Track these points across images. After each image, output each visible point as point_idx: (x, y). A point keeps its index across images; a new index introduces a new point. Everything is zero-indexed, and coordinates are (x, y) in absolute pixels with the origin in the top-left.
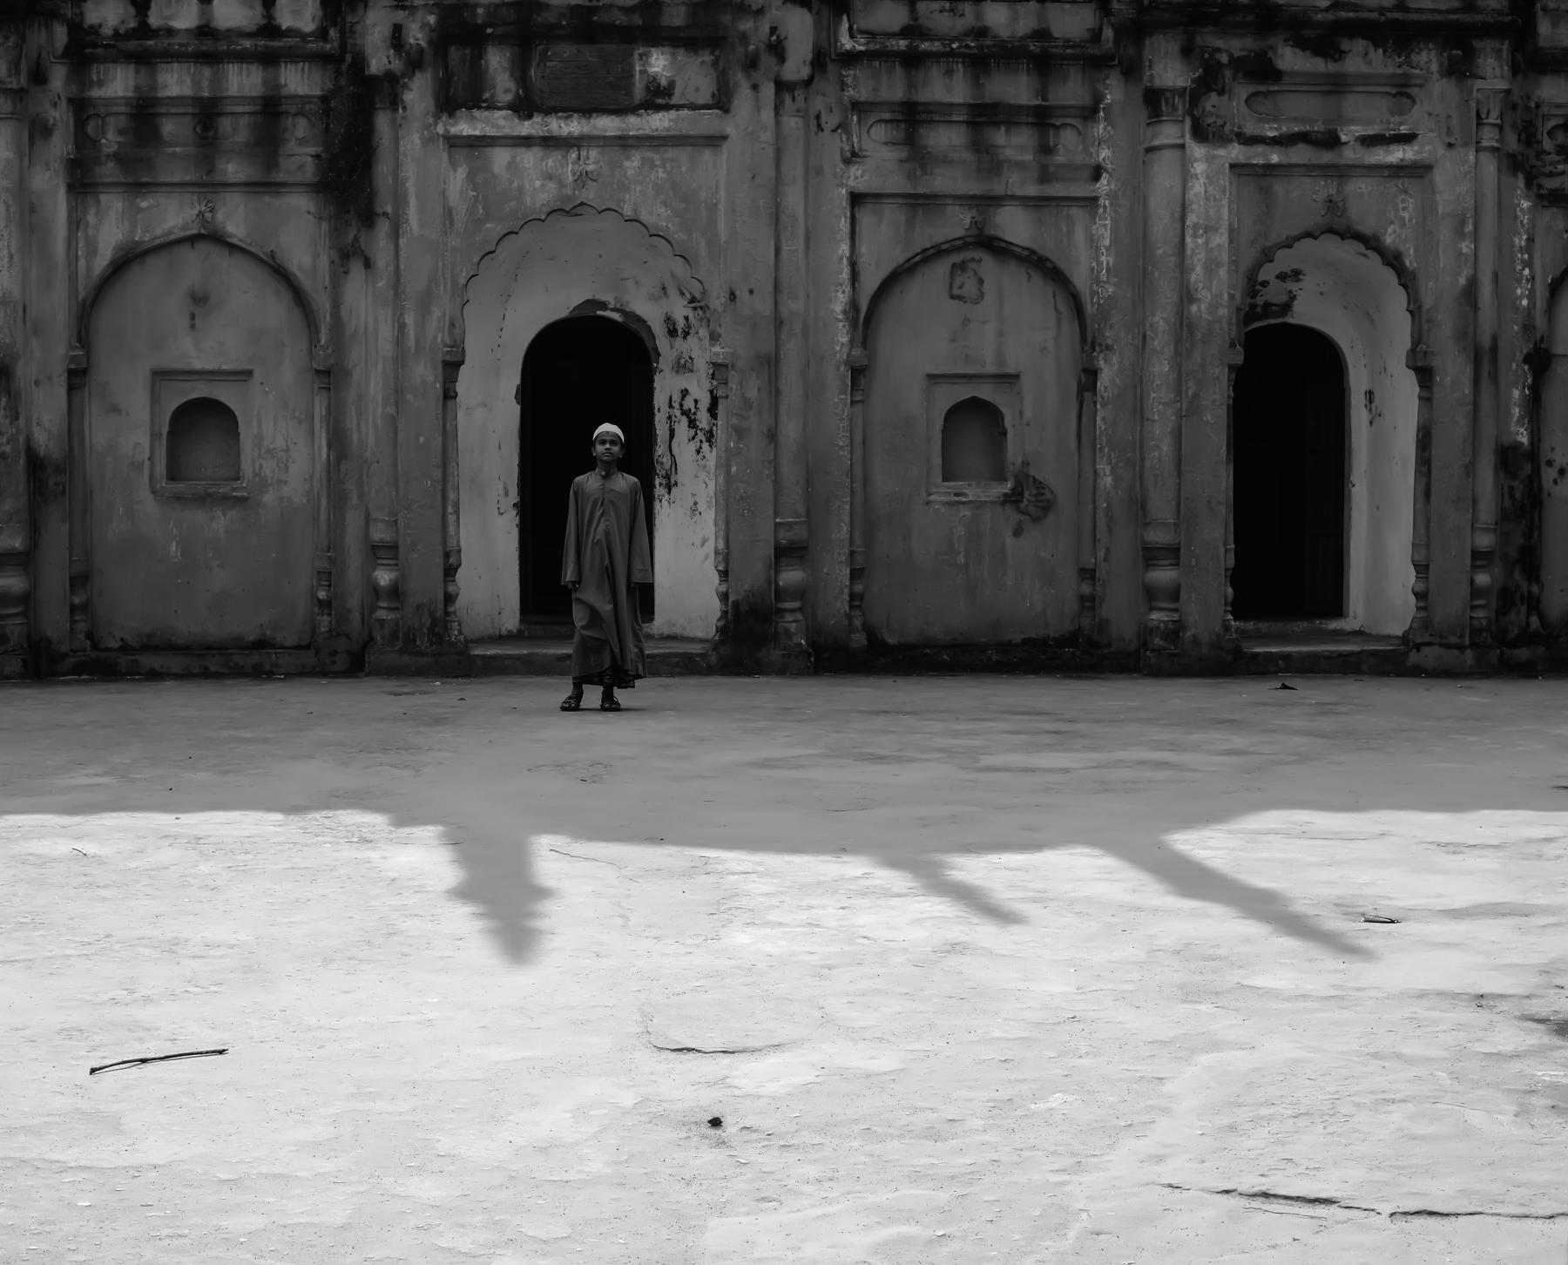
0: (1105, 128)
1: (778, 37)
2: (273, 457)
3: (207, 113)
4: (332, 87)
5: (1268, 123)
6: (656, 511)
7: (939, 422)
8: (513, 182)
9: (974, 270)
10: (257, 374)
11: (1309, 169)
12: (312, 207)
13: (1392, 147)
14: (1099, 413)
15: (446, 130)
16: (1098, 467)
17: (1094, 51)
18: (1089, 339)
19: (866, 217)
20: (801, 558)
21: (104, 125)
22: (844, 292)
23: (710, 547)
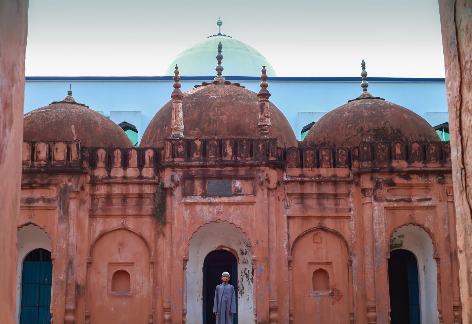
1: (268, 177)
2: (139, 285)
3: (125, 197)
4: (156, 191)
5: (393, 196)
7: (312, 275)
9: (319, 235)
10: (135, 264)
11: (405, 208)
12: (150, 221)
13: (425, 202)
14: (353, 272)
15: (185, 201)
16: (353, 286)
17: (348, 179)
19: (291, 222)
20: (276, 311)
21: (98, 200)
22: (286, 241)
23: (252, 309)
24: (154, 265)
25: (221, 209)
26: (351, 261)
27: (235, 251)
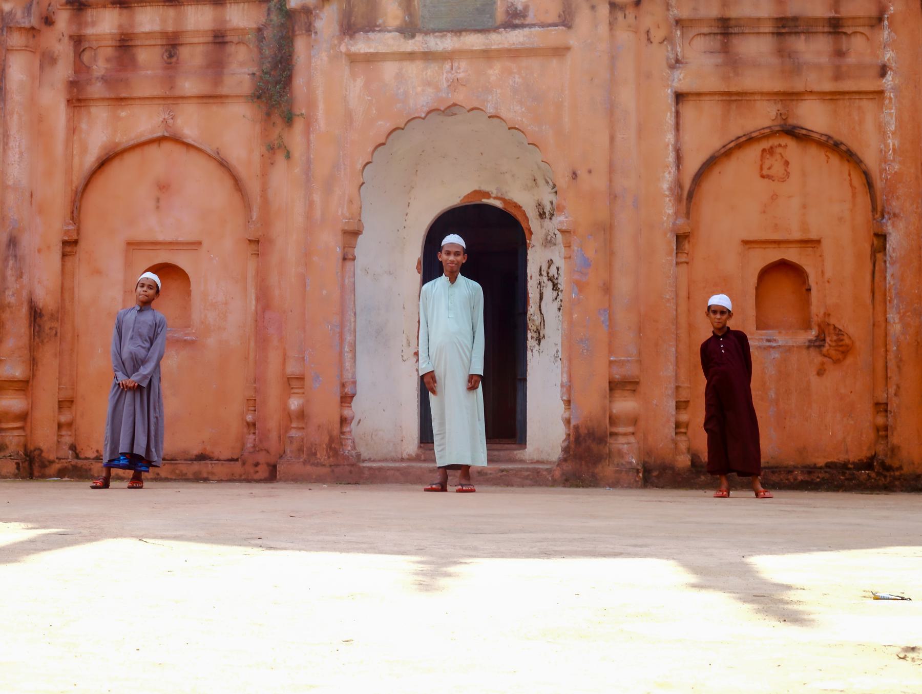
0: (889, 34)
6: (528, 359)
7: (754, 280)
8: (399, 89)
9: (781, 154)
14: (888, 270)
15: (348, 50)
16: (888, 316)
18: (879, 209)
19: (689, 110)
21: (95, 55)
22: (670, 173)
24: (258, 248)
25: (461, 70)
26: (882, 237)
27: (520, 207)
